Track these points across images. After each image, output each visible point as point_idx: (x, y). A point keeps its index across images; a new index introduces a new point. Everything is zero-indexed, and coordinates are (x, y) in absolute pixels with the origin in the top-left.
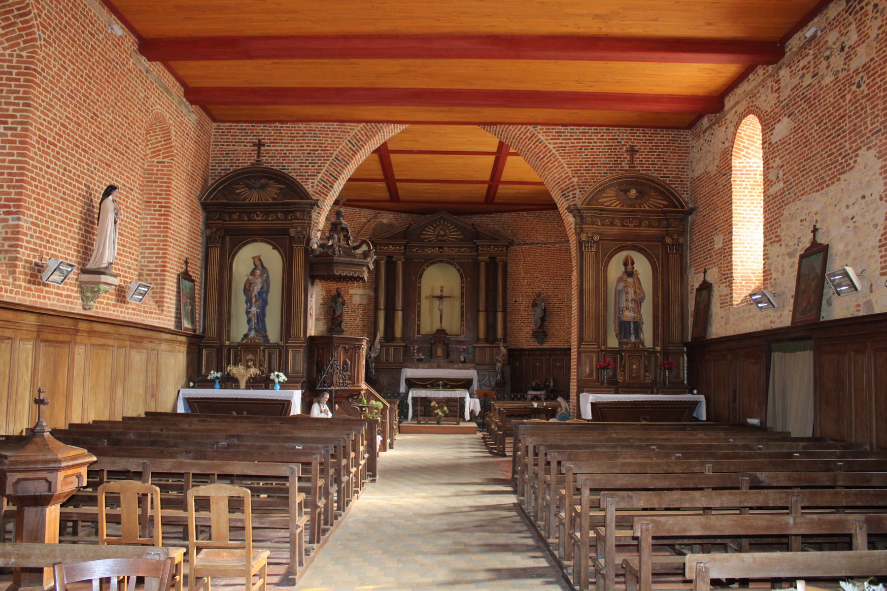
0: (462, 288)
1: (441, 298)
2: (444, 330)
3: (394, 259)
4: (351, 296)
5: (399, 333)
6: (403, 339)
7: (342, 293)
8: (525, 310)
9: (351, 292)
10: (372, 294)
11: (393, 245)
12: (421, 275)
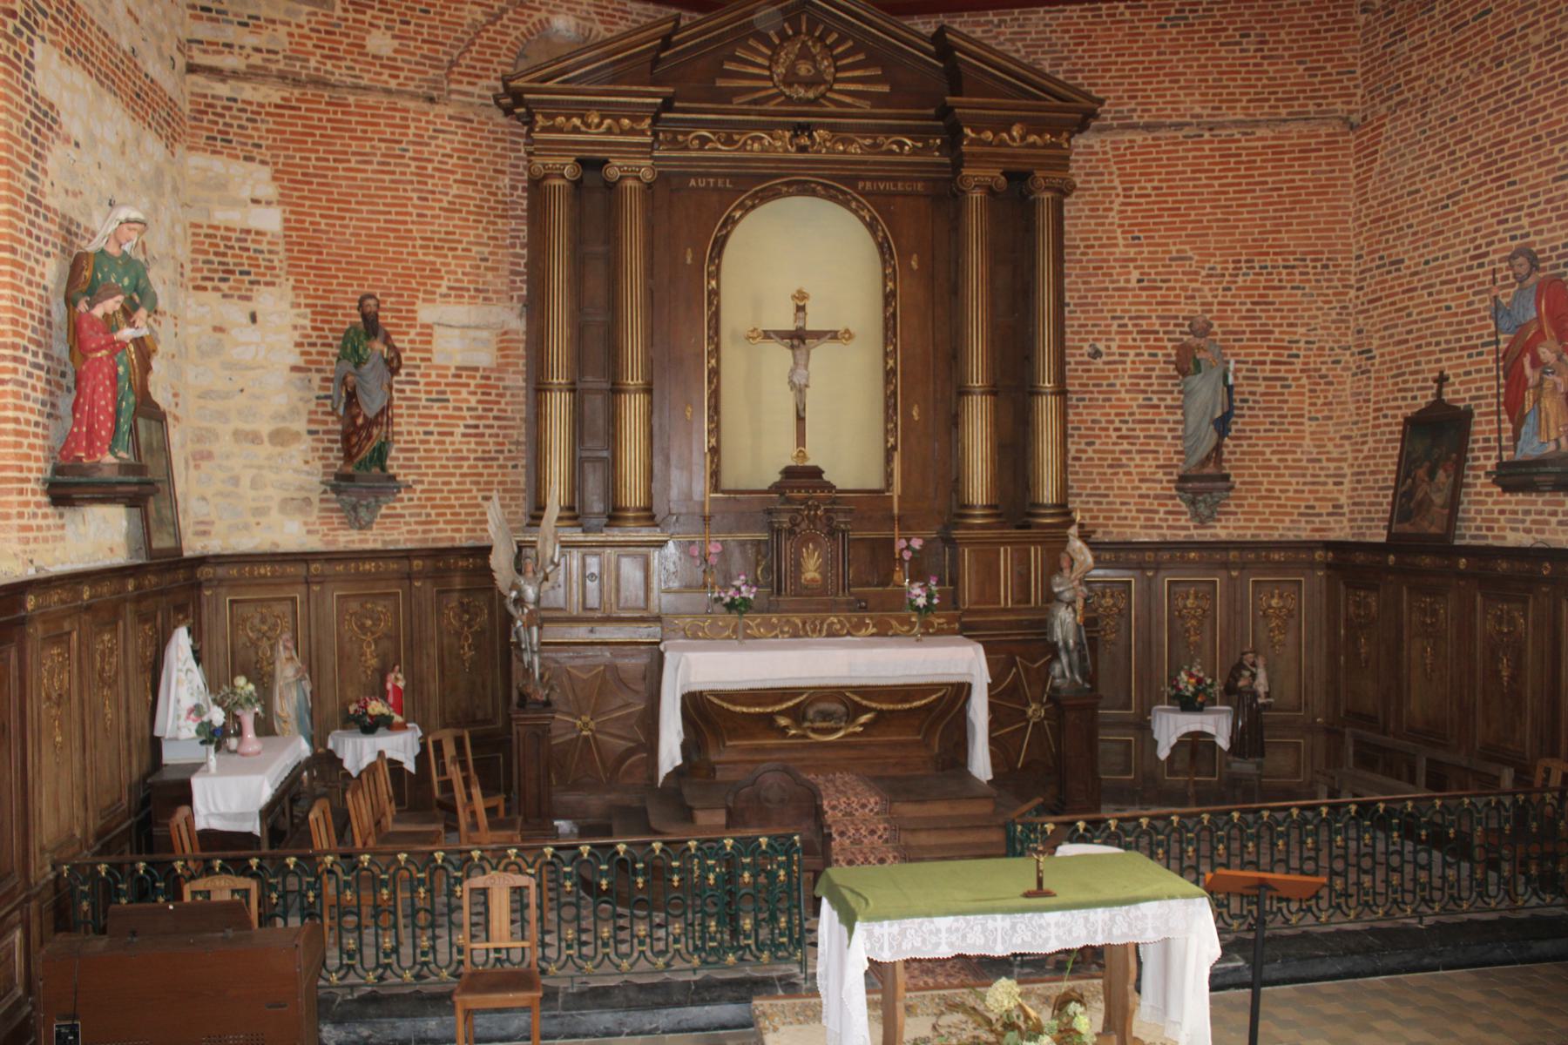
0: (888, 298)
1: (798, 338)
2: (816, 472)
3: (613, 172)
4: (427, 331)
7: (386, 318)
8: (1134, 389)
10: (517, 324)
11: (606, 111)
12: (720, 244)
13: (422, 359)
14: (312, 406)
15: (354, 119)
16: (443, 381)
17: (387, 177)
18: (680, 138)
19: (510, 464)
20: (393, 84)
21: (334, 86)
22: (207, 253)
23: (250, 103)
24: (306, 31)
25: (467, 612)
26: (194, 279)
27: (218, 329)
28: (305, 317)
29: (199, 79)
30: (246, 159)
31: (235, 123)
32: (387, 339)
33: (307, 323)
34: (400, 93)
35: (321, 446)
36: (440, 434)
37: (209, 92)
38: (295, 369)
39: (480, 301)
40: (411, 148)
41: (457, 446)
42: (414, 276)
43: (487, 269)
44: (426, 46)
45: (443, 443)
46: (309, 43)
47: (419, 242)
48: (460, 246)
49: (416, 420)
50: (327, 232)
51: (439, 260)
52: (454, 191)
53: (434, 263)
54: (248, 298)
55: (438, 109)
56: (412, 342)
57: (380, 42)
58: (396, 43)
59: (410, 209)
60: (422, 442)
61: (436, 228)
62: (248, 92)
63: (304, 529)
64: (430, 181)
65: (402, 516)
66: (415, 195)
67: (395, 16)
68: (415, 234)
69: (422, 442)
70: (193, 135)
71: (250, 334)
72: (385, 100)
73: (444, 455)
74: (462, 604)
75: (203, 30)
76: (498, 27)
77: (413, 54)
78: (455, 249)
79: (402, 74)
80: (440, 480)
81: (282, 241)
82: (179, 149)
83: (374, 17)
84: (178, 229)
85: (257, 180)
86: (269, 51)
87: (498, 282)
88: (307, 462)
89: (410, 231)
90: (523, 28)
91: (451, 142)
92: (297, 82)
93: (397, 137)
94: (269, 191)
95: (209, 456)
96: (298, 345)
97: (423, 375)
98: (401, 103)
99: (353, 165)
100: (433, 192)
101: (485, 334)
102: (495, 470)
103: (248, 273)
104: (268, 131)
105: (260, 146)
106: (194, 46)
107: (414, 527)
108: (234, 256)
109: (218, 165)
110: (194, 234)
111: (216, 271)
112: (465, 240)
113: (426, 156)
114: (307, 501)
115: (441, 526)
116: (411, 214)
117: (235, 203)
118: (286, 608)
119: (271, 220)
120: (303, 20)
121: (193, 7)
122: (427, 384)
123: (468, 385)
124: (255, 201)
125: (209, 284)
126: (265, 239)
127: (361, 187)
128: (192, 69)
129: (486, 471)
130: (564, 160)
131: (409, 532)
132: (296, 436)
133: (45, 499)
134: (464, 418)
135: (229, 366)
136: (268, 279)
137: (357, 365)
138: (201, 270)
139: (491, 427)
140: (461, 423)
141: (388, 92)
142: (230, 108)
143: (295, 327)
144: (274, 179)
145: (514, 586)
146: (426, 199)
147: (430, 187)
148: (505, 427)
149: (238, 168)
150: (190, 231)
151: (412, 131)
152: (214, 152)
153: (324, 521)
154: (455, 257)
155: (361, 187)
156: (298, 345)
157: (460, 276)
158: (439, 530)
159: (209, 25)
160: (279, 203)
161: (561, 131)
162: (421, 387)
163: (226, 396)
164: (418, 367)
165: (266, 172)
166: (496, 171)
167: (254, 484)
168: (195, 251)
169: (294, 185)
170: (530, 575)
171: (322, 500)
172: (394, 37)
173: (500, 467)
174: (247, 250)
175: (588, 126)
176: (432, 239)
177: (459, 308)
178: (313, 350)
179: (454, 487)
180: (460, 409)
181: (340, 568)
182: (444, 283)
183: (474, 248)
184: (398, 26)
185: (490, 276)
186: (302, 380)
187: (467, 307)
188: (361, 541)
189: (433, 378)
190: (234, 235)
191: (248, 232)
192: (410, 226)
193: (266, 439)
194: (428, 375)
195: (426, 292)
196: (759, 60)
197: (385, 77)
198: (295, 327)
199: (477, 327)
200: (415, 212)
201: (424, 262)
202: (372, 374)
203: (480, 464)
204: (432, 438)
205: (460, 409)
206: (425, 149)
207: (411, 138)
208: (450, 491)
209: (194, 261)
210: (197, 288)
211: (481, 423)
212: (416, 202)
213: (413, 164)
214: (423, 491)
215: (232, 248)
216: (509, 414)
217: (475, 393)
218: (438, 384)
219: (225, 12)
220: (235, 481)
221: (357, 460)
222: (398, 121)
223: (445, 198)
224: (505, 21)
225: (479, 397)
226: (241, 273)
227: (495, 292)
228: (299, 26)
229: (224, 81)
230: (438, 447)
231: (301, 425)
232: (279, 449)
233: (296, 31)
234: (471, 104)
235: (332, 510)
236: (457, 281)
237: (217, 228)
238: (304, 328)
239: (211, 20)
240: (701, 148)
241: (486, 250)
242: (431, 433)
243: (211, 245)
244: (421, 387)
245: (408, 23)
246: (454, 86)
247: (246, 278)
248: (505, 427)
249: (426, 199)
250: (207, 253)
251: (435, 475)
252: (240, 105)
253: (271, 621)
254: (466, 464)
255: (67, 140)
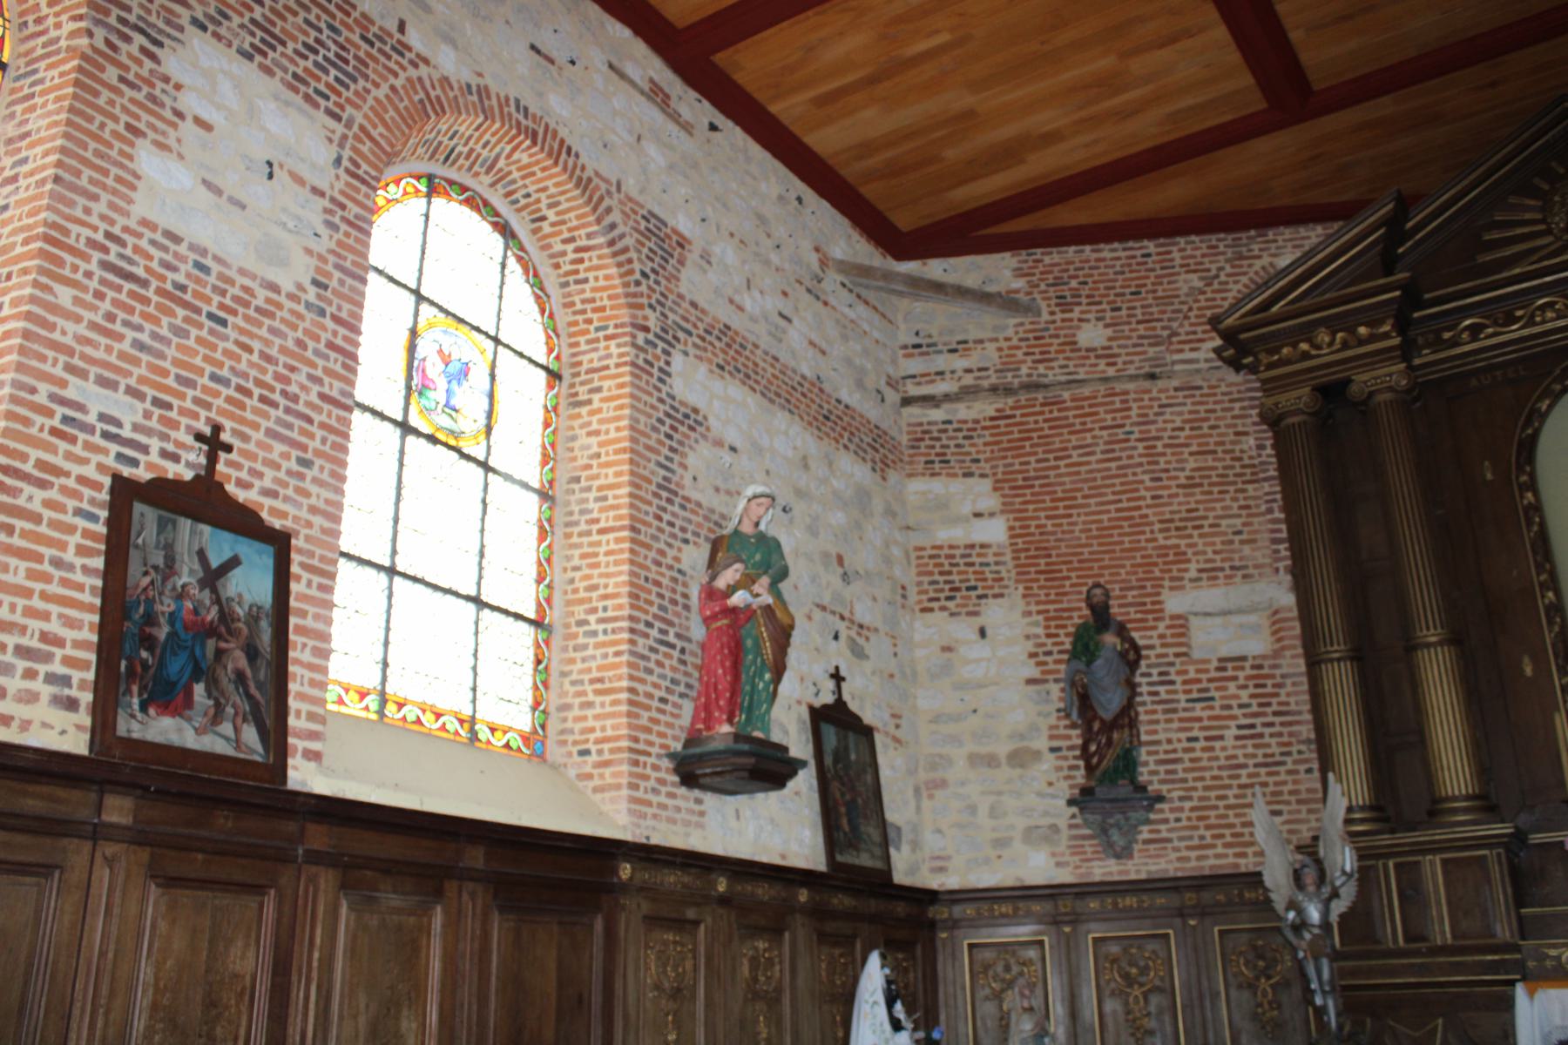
4: (1181, 624)
5: (1454, 771)
6: (1486, 805)
9: (1174, 603)
10: (1288, 599)
11: (1332, 325)
12: (1528, 448)
13: (1177, 655)
14: (1053, 721)
15: (1071, 413)
16: (1204, 676)
17: (1113, 465)
18: (1447, 335)
19: (1302, 768)
20: (1111, 372)
21: (1046, 386)
22: (931, 573)
23: (965, 422)
24: (1015, 342)
25: (1261, 957)
26: (920, 602)
27: (947, 649)
28: (1036, 624)
29: (914, 412)
30: (966, 475)
31: (952, 443)
32: (1122, 631)
33: (1040, 631)
34: (1117, 379)
35: (1065, 764)
36: (1207, 739)
37: (925, 420)
38: (1030, 681)
39: (1238, 579)
40: (1136, 429)
41: (1230, 752)
42: (1156, 564)
43: (1242, 542)
44: (1141, 327)
45: (1212, 749)
46: (1019, 353)
47: (1157, 526)
48: (1206, 523)
49: (1176, 725)
50: (1054, 533)
51: (1183, 542)
52: (1192, 464)
53: (1178, 546)
54: (975, 614)
55: (1160, 384)
56: (1161, 636)
57: (1092, 335)
58: (1109, 332)
59: (1143, 493)
60: (1186, 750)
61: (1175, 508)
62: (963, 412)
63: (1052, 861)
64: (1162, 460)
65: (1169, 840)
66: (1146, 477)
67: (1104, 306)
68: (1152, 518)
69: (1186, 750)
70: (911, 463)
71: (980, 650)
72: (1102, 388)
73: (1215, 764)
74: (1255, 948)
75: (915, 366)
76: (1216, 286)
77: (1129, 338)
78: (1201, 527)
79: (1120, 360)
80: (1213, 794)
81: (1008, 551)
82: (893, 476)
83: (1082, 312)
84: (896, 552)
85: (980, 492)
86: (980, 370)
87: (1261, 555)
88: (1050, 784)
89: (1146, 516)
90: (1244, 279)
91: (1180, 414)
92: (1009, 391)
93: (1119, 422)
94: (991, 502)
95: (943, 784)
96: (1032, 655)
97: (1178, 673)
98: (1119, 387)
99: (1075, 459)
100: (1167, 471)
101: (1253, 618)
102: (1283, 777)
103: (975, 588)
104: (986, 444)
105: (977, 461)
106: (908, 381)
107: (1185, 853)
108: (959, 573)
109: (937, 486)
110: (919, 558)
111: (942, 590)
112: (1211, 514)
113: (1154, 434)
114: (1054, 828)
115: (1220, 850)
116: (1144, 498)
117: (957, 520)
118: (1032, 953)
119: (995, 532)
120: (1010, 332)
121: (905, 347)
122: (1185, 682)
123: (1235, 678)
124: (978, 515)
125: (935, 605)
126: (990, 551)
127: (1086, 481)
128: (907, 401)
129: (1271, 780)
130: (1295, 394)
131: (1180, 859)
132: (1037, 755)
133: (676, 779)
134: (1234, 718)
135: (961, 686)
136: (996, 591)
137: (1089, 663)
138: (926, 592)
139: (1271, 725)
140: (1233, 723)
141: (1106, 380)
142: (945, 431)
143: (1028, 637)
144: (995, 489)
145: (1292, 905)
146: (1160, 479)
147: (1162, 466)
148: (1290, 724)
149: (957, 486)
150: (913, 555)
151: (1134, 413)
152: (933, 475)
153: (1076, 850)
154: (1201, 536)
155: (1086, 481)
156: (1032, 655)
157: (1211, 556)
158: (1217, 856)
159: (921, 359)
160: (1002, 512)
161: (1288, 362)
162: (1178, 687)
163: (957, 718)
164: (1172, 664)
165: (987, 484)
166: (1237, 434)
167: (993, 813)
168: (920, 574)
169: (1014, 490)
170: (1311, 889)
171: (1071, 826)
172: (1107, 326)
173: (1289, 772)
174: (972, 564)
175: (1319, 348)
176: (1171, 521)
177: (1215, 591)
178: (1049, 659)
179: (1232, 801)
180: (1229, 707)
181: (1094, 904)
182: (1193, 566)
183: (1224, 522)
184: (1109, 314)
185: (1247, 550)
186: (1039, 693)
187: (1223, 590)
188: (1120, 873)
189: (1192, 675)
190: (958, 552)
191: (972, 546)
192: (1144, 511)
193: (1003, 761)
194: (1186, 672)
195: (1172, 579)
196: (1528, 216)
197: (1102, 367)
198: (1028, 637)
199: (1240, 611)
200: (1148, 494)
201: (1166, 547)
202: (1104, 669)
203: (1263, 771)
204: (1198, 745)
205: (1229, 707)
206: (1152, 427)
207: (1135, 419)
208: (1228, 807)
209: (919, 584)
210: (924, 610)
211: (1258, 721)
212: (1149, 484)
213: (1140, 445)
214: (1192, 809)
215: (957, 565)
216: (1293, 707)
217: (1245, 687)
218: (1199, 681)
219: (934, 345)
220: (973, 809)
221: (1098, 773)
222: (1118, 405)
223: (1181, 474)
224: (1223, 278)
225: (1252, 690)
226: (968, 589)
227: (1256, 567)
228: (1007, 339)
229: (937, 406)
230: (1206, 755)
231: (1042, 743)
232: (1018, 771)
233: (1005, 345)
234: (1198, 371)
235: (1084, 837)
236: (1207, 561)
237: (940, 547)
238: (1037, 636)
239: (922, 354)
240: (1474, 339)
241: (1238, 522)
242: (1196, 739)
243: (936, 565)
244: (1178, 687)
245: (1119, 309)
246: (1177, 357)
247: (973, 593)
248: (1290, 724)
249: (1160, 479)
250: (931, 573)
251: (1206, 788)
252: (955, 426)
253: (1015, 969)
254: (1244, 772)
255: (718, 443)
